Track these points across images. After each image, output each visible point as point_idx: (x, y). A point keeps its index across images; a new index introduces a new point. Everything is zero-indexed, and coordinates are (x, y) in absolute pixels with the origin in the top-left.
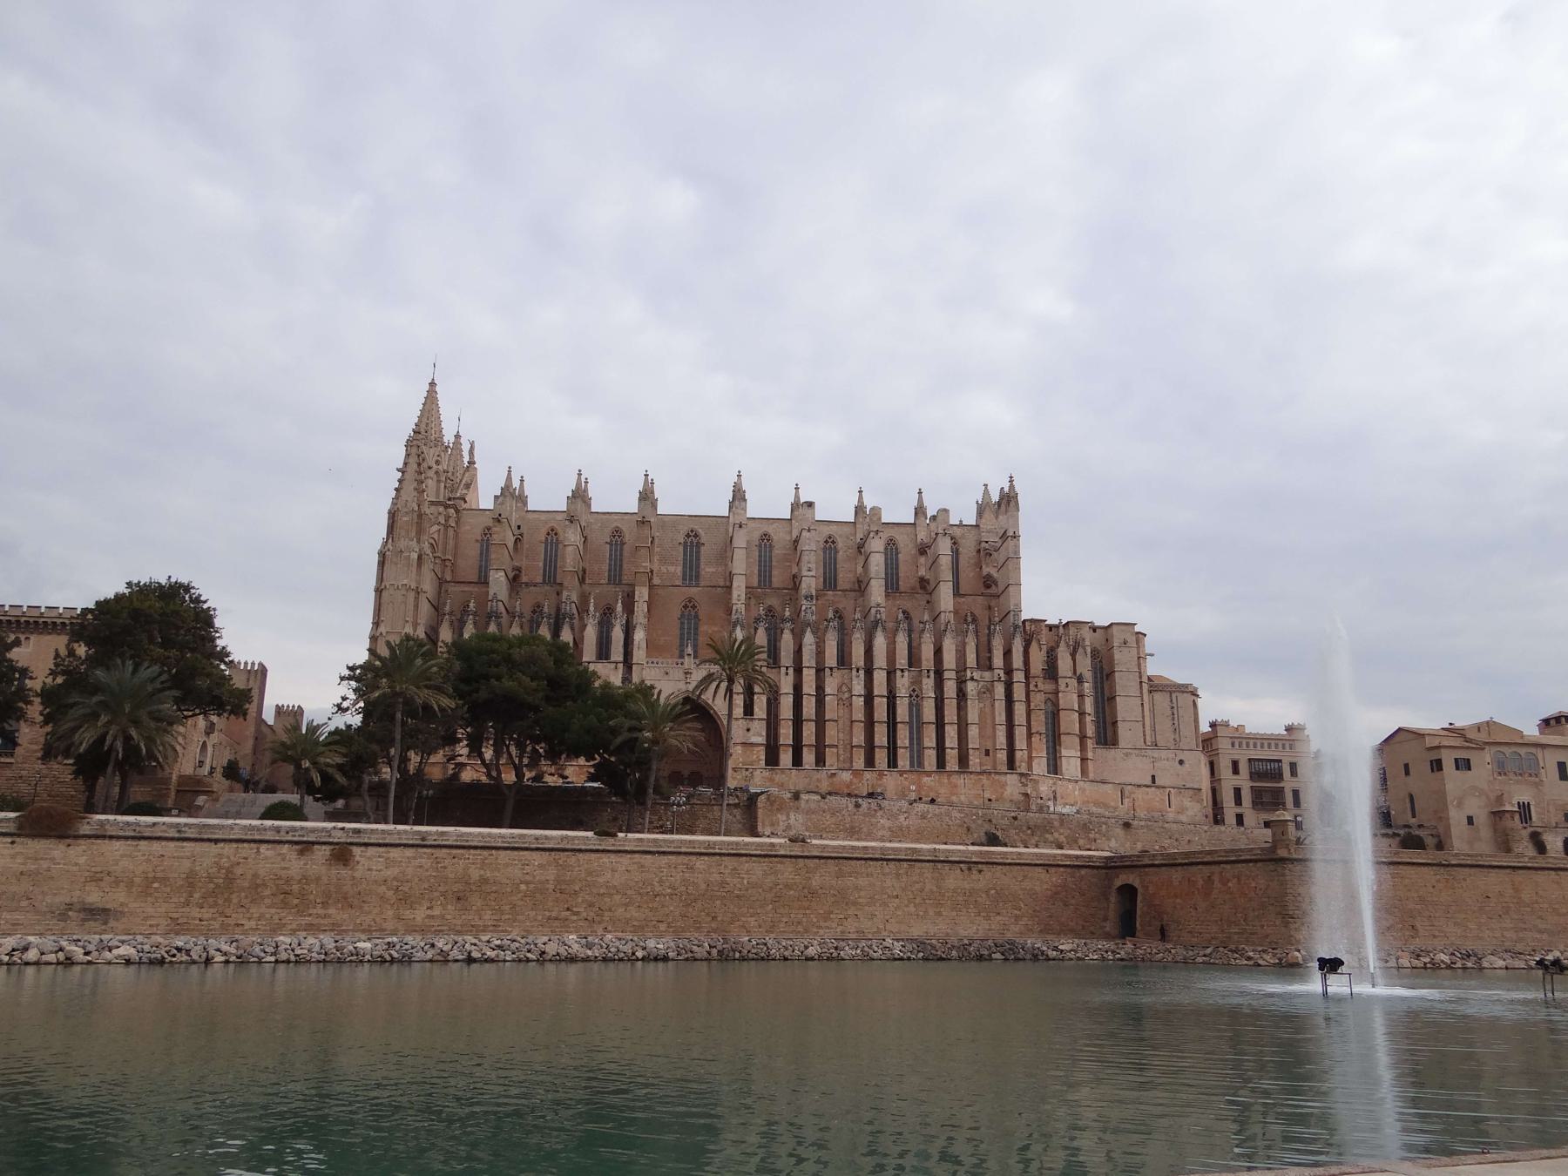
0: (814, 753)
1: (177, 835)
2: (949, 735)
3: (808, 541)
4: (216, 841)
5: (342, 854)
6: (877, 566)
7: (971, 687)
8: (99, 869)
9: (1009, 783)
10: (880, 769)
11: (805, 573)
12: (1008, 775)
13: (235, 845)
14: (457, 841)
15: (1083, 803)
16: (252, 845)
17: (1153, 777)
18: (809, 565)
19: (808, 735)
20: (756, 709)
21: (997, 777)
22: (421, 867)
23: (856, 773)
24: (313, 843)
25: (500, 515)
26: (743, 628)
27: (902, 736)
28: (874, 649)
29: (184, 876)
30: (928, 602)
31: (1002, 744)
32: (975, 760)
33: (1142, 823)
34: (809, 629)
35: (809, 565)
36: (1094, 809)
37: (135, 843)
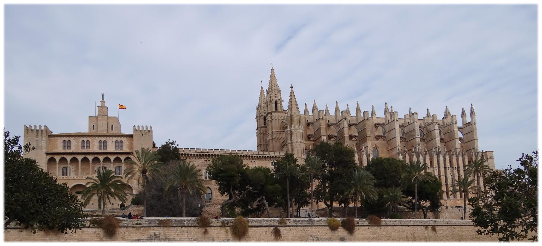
1: (401, 224)
3: (417, 126)
4: (409, 226)
5: (434, 229)
6: (437, 134)
8: (388, 236)
11: (417, 136)
13: (412, 227)
14: (454, 223)
16: (416, 227)
18: (418, 134)
22: (449, 232)
24: (427, 225)
25: (322, 117)
26: (402, 155)
28: (440, 161)
29: (405, 237)
30: (445, 145)
34: (421, 155)
35: (418, 134)
37: (393, 227)
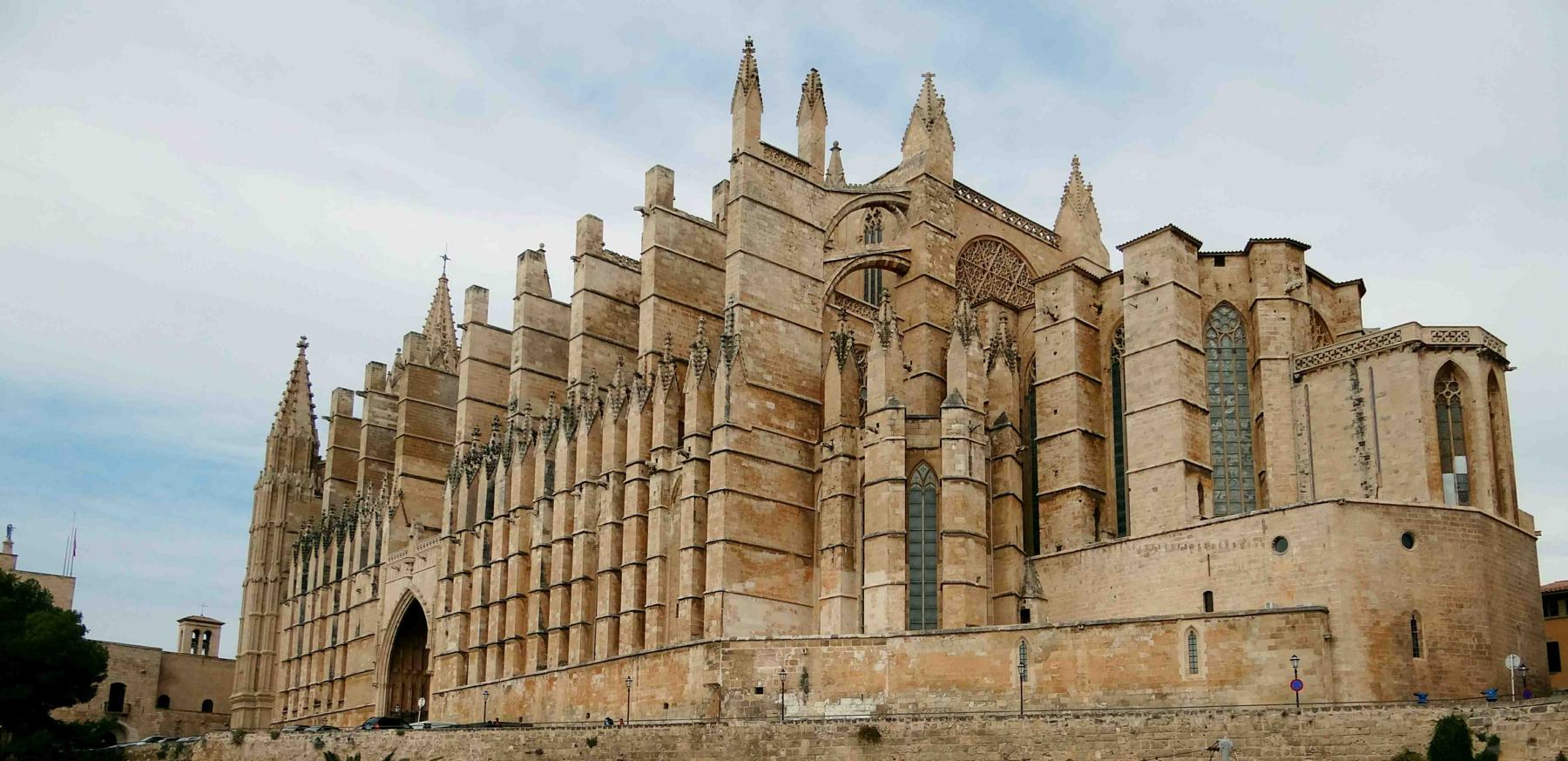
0: (495, 658)
2: (625, 588)
7: (655, 482)
9: (691, 666)
10: (552, 669)
12: (691, 649)
15: (901, 687)
17: (1208, 596)
19: (492, 627)
20: (454, 600)
21: (676, 657)
23: (530, 686)
27: (576, 605)
31: (685, 587)
32: (652, 629)
33: (921, 725)
36: (931, 701)
